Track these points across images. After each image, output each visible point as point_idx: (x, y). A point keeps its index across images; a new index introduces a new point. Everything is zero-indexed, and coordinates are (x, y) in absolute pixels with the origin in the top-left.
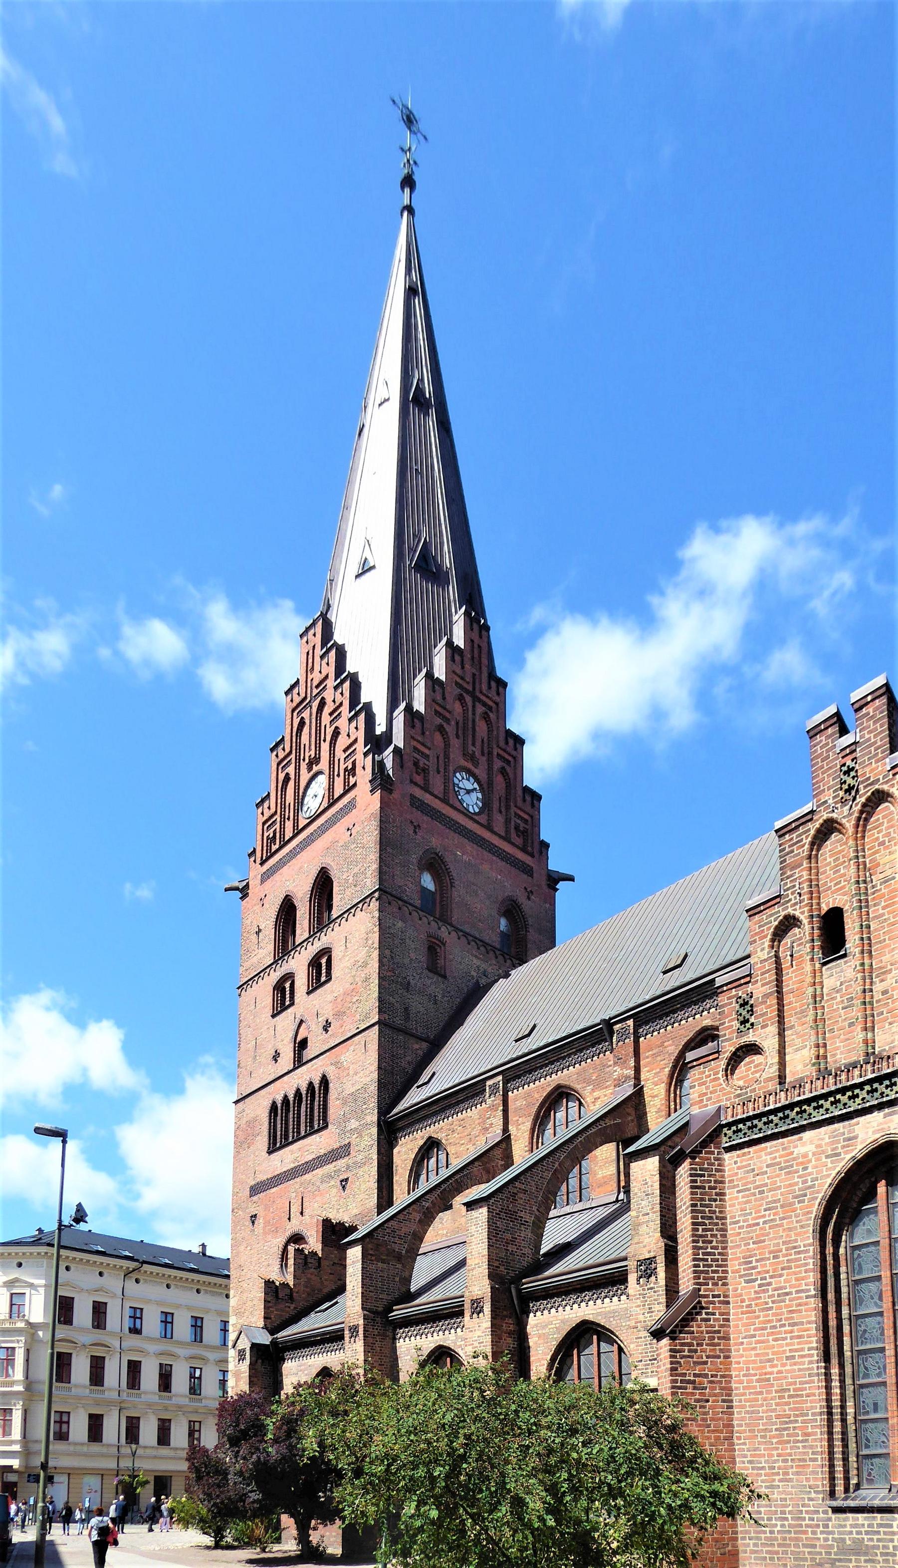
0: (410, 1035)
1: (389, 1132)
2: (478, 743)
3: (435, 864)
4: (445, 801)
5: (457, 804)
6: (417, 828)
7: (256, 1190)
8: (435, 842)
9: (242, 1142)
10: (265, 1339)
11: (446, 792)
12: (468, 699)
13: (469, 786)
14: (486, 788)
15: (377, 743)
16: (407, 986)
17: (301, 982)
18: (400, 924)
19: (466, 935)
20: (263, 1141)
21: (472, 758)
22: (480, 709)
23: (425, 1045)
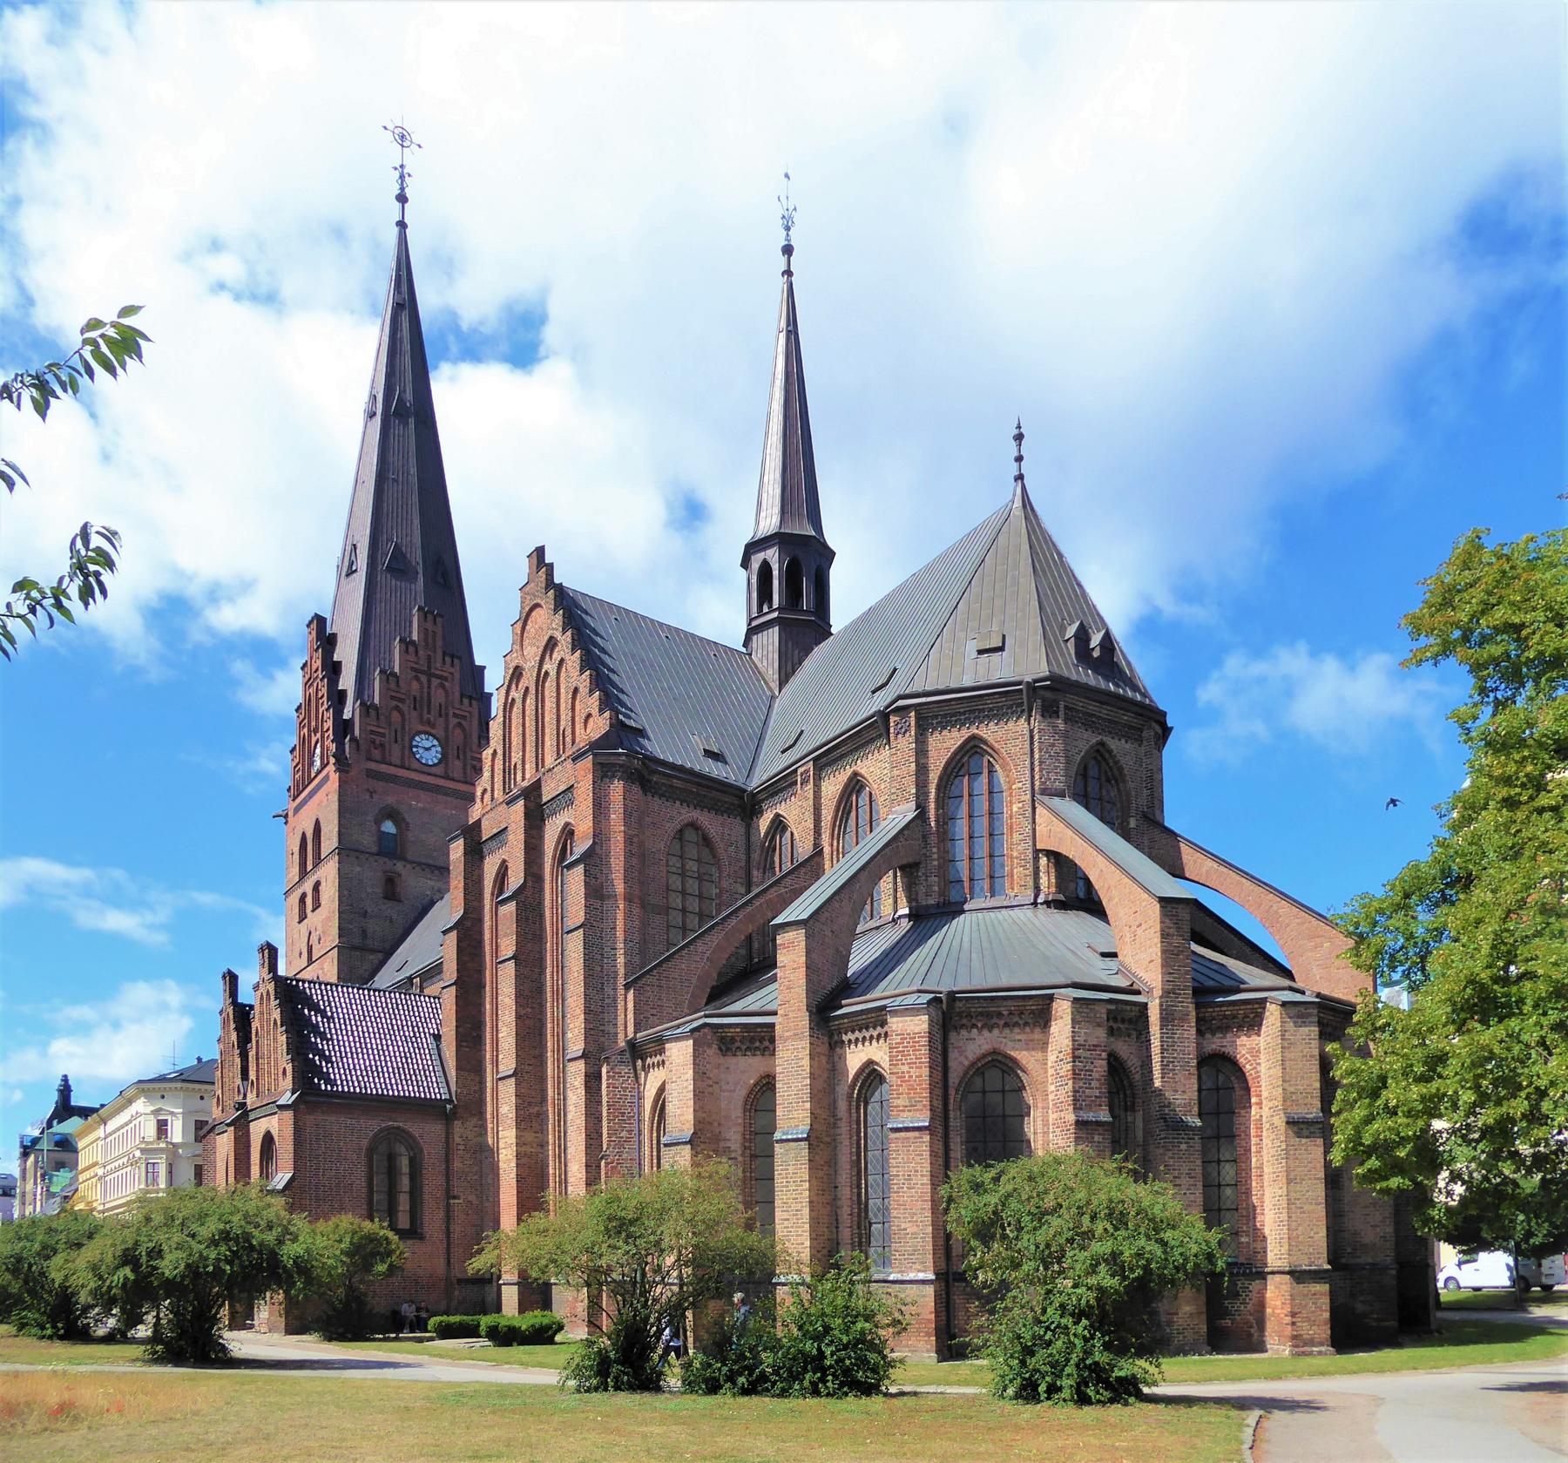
2: (435, 711)
4: (402, 767)
5: (415, 765)
6: (371, 793)
8: (390, 800)
11: (402, 759)
12: (424, 679)
13: (427, 744)
14: (444, 744)
15: (342, 728)
16: (365, 914)
19: (419, 864)
21: (429, 723)
22: (435, 682)
23: (380, 956)
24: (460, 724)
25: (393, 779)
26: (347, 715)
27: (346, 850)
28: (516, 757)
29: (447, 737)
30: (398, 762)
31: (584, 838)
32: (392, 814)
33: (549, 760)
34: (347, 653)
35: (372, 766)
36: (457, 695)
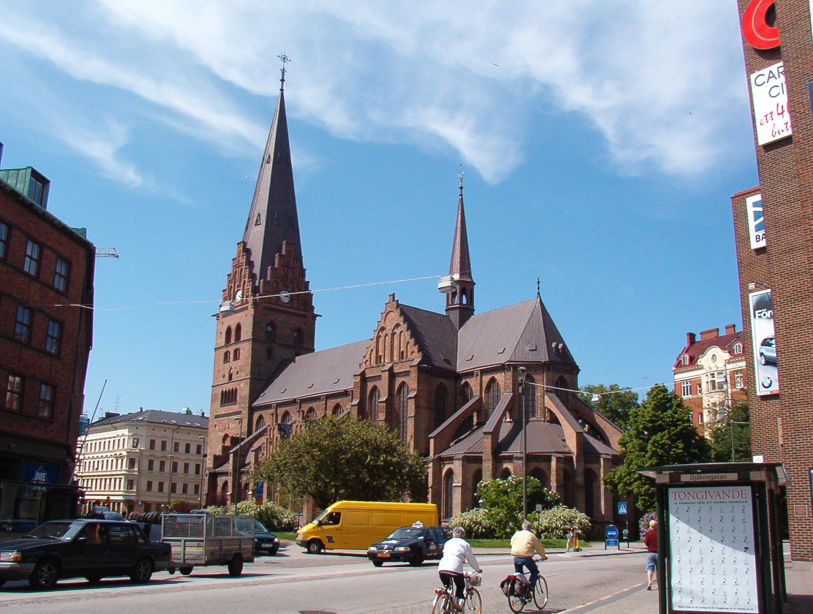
0: (261, 380)
1: (252, 410)
3: (272, 324)
7: (217, 417)
9: (213, 400)
10: (213, 471)
17: (232, 356)
20: (219, 402)
21: (287, 286)
26: (257, 284)
27: (255, 340)
28: (380, 353)
31: (414, 390)
32: (272, 324)
33: (396, 359)
34: (257, 257)
35: (266, 305)
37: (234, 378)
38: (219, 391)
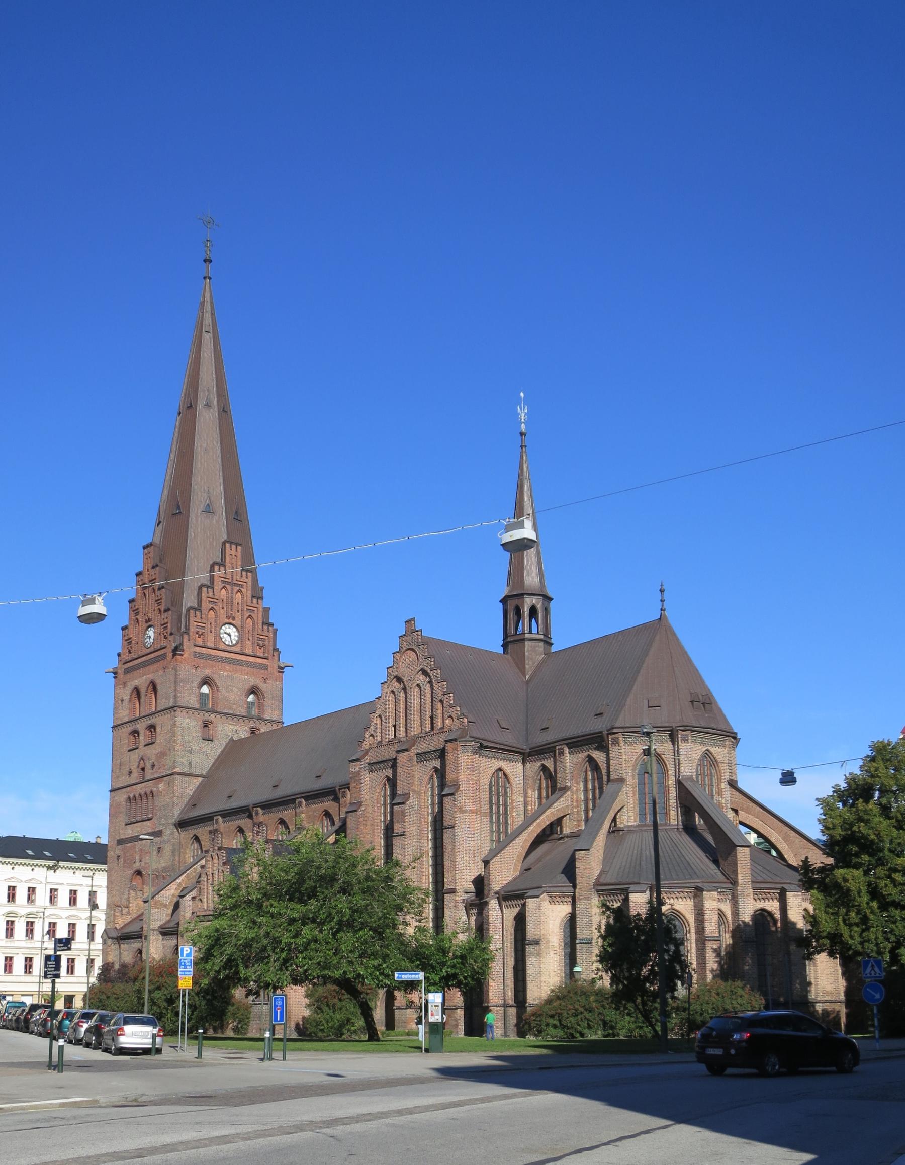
5: (222, 647)
8: (207, 672)
16: (191, 752)
18: (187, 720)
24: (250, 617)
25: (209, 657)
29: (242, 627)
30: (212, 645)
32: (206, 681)
35: (198, 649)
36: (250, 596)
37: (149, 774)
38: (122, 797)
